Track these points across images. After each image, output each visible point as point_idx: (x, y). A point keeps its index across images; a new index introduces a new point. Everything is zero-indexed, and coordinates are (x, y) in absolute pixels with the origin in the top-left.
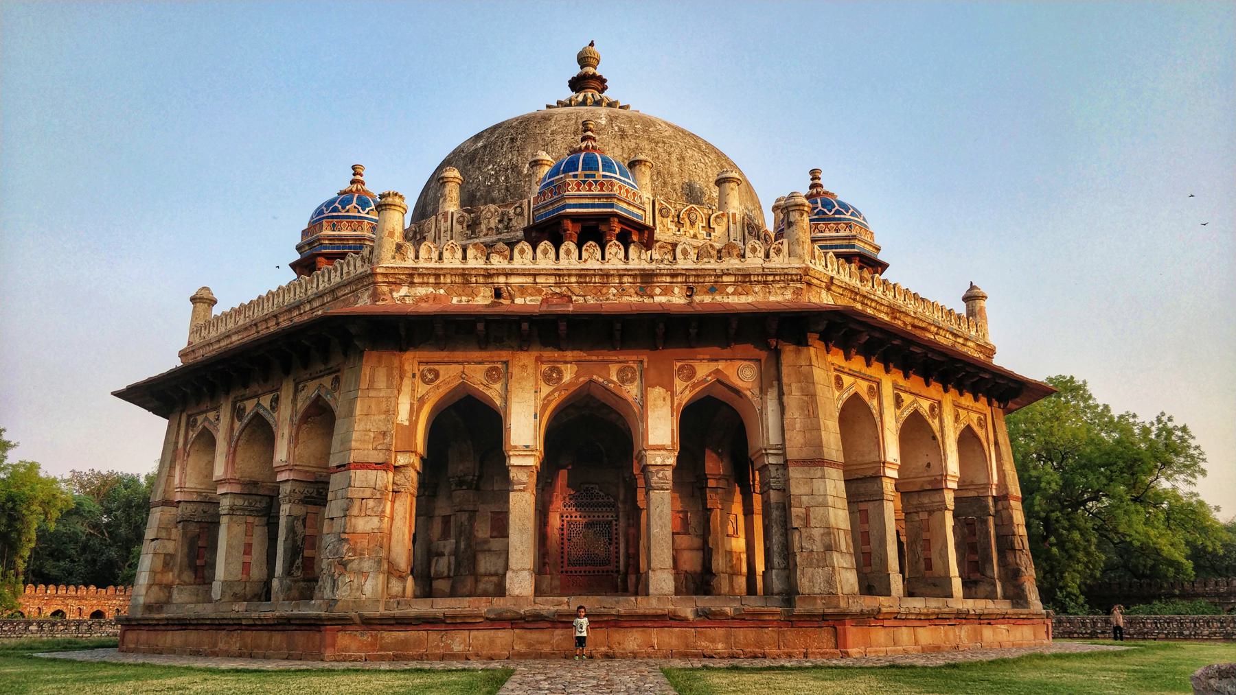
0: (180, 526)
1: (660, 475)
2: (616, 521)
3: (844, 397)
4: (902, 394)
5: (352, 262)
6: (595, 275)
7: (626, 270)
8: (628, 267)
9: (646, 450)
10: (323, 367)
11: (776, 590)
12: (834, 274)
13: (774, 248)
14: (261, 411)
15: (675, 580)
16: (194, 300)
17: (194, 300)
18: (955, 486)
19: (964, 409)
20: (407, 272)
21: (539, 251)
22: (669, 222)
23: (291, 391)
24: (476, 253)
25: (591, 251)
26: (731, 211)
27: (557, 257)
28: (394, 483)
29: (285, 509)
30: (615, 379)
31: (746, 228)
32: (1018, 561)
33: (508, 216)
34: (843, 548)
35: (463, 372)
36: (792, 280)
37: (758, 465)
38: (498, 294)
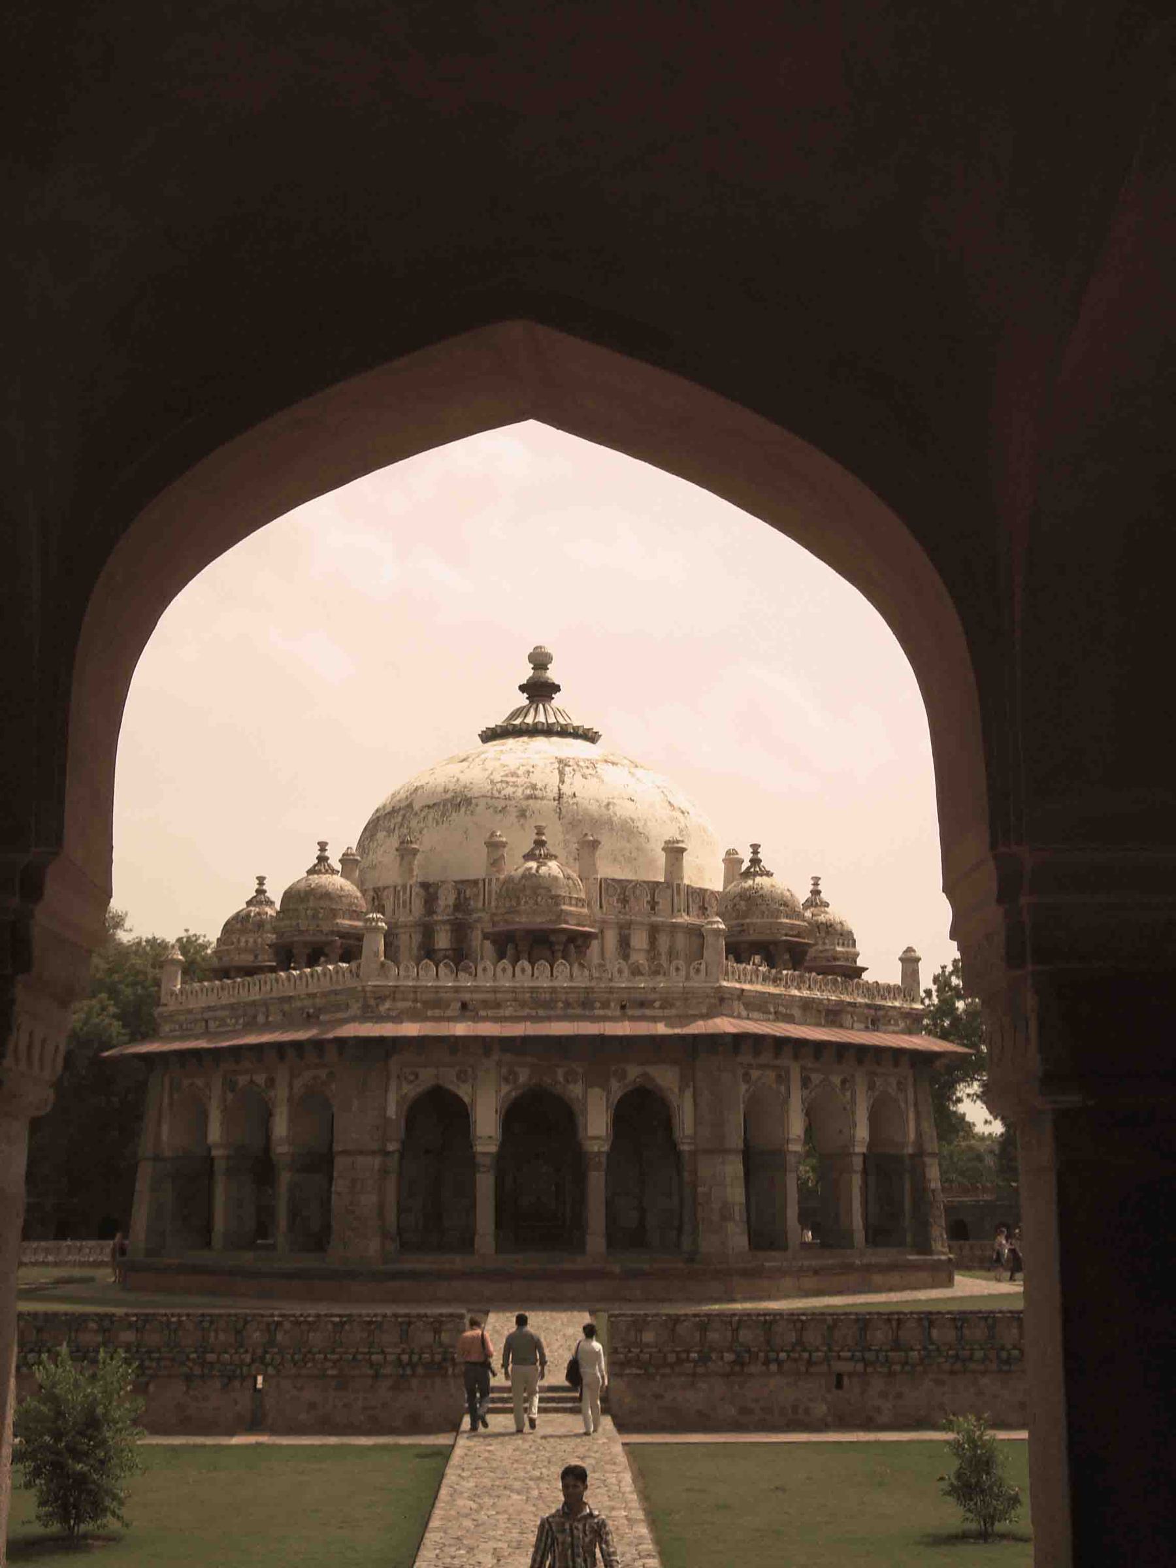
1: (597, 1159)
7: (571, 988)
8: (573, 984)
12: (747, 987)
18: (864, 1150)
21: (499, 970)
27: (514, 975)
29: (285, 1178)
34: (737, 1218)
37: (677, 1148)
38: (464, 1006)
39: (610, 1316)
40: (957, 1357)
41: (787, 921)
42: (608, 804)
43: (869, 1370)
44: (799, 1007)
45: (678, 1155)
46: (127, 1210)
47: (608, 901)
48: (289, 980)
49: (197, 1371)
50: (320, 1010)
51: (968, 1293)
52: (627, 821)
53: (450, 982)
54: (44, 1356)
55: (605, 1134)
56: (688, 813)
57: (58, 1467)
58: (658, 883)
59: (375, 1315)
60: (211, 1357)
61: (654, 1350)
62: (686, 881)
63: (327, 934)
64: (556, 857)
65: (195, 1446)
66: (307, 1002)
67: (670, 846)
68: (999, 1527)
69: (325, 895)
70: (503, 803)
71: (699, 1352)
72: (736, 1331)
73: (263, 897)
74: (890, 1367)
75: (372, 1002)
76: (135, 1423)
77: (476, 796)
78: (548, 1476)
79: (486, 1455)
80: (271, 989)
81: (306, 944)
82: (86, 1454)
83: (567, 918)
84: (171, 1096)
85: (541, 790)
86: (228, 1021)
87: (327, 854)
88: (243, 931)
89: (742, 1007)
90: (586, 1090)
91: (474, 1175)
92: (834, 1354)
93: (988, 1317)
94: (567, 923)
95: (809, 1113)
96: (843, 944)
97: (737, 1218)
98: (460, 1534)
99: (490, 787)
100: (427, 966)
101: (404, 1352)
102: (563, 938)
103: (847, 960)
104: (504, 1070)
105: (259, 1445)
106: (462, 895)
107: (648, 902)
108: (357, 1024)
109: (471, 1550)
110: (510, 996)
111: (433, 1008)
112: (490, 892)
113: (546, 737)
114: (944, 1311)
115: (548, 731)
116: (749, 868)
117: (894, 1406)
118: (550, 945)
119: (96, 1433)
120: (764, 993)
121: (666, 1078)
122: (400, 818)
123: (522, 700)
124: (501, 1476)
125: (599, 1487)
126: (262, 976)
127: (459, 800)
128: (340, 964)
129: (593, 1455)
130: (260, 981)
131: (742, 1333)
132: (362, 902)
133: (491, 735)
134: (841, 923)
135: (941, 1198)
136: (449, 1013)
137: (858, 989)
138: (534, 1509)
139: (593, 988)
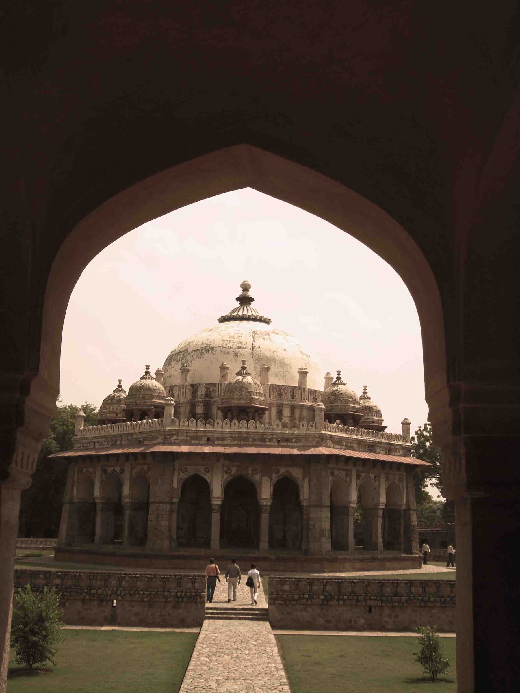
4: (361, 474)
5: (154, 423)
12: (334, 434)
14: (115, 473)
18: (383, 507)
22: (276, 394)
25: (243, 424)
27: (231, 426)
28: (172, 508)
29: (127, 513)
30: (251, 473)
31: (310, 393)
34: (327, 536)
35: (196, 469)
38: (209, 439)
39: (270, 578)
40: (422, 600)
41: (352, 405)
42: (274, 352)
43: (383, 604)
44: (357, 443)
45: (301, 507)
46: (58, 526)
48: (131, 425)
49: (87, 598)
50: (145, 439)
51: (428, 572)
52: (282, 360)
53: (202, 428)
54: (20, 590)
55: (269, 497)
56: (309, 356)
57: (25, 639)
58: (295, 387)
59: (166, 575)
60: (93, 591)
61: (289, 593)
62: (308, 386)
63: (149, 406)
64: (250, 374)
65: (86, 630)
66: (139, 436)
67: (301, 370)
68: (439, 676)
69: (149, 389)
70: (228, 350)
71: (308, 595)
72: (325, 586)
73: (121, 388)
74: (393, 604)
75: (168, 437)
76: (60, 619)
77: (216, 346)
78: (241, 648)
79: (214, 638)
80: (124, 430)
81: (139, 410)
82: (38, 633)
83: (254, 402)
84: (78, 476)
85: (245, 344)
86: (104, 443)
87: (149, 370)
88: (111, 404)
89: (331, 442)
90: (262, 478)
91: (211, 514)
92: (368, 597)
93: (436, 583)
94: (255, 404)
95: (360, 490)
96: (377, 416)
97: (327, 536)
98: (202, 672)
99: (222, 343)
100: (192, 422)
101: (178, 592)
102: (253, 410)
103: (378, 423)
104: (225, 468)
105: (114, 631)
106: (209, 391)
107: (290, 395)
108: (161, 446)
109: (206, 680)
110: (229, 435)
111: (195, 440)
112: (221, 389)
113: (247, 321)
114: (417, 580)
115: (248, 318)
116: (336, 381)
117: (394, 621)
118: (247, 413)
119: (42, 624)
120: (341, 437)
121: (297, 473)
122: (182, 356)
123: (237, 304)
124: (220, 647)
125: (263, 653)
126: (120, 424)
127: (208, 348)
128: (154, 419)
129: (261, 639)
130: (119, 426)
131: (327, 587)
132: (164, 392)
133: (223, 320)
134: (376, 407)
135: (417, 529)
136: (202, 442)
138: (235, 662)
139: (265, 433)
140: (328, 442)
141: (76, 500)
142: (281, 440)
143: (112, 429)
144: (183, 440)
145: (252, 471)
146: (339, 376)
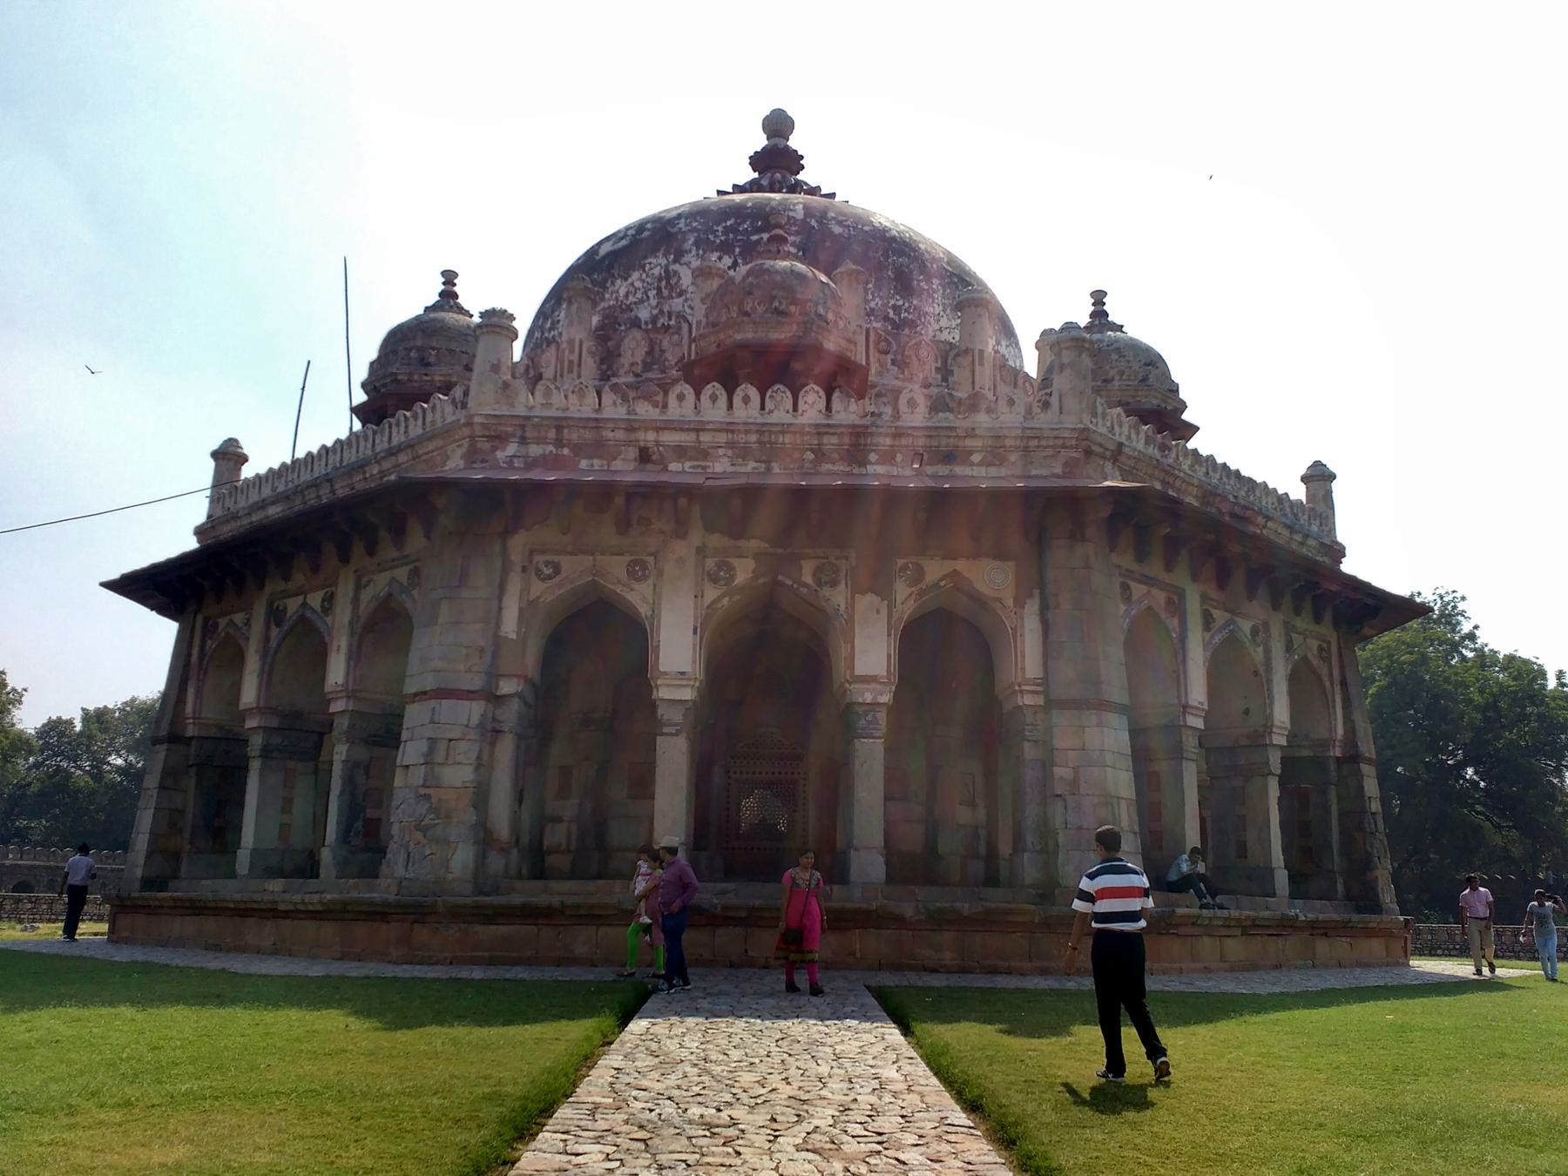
0: (193, 771)
1: (869, 718)
2: (805, 780)
3: (1133, 612)
4: (1216, 613)
5: (438, 406)
6: (783, 432)
7: (828, 425)
9: (850, 683)
10: (395, 554)
11: (1028, 880)
12: (1123, 439)
13: (1039, 401)
14: (308, 614)
15: (887, 863)
16: (215, 455)
17: (215, 455)
19: (1300, 633)
20: (517, 423)
22: (889, 361)
23: (351, 586)
24: (614, 397)
26: (979, 347)
27: (730, 406)
28: (494, 719)
29: (340, 753)
32: (1369, 849)
33: (660, 346)
35: (594, 566)
36: (1064, 447)
38: (644, 456)
47: (879, 360)
66: (386, 465)
90: (853, 597)
104: (710, 563)
106: (657, 349)
107: (937, 369)
111: (591, 458)
137: (1266, 497)
140: (1106, 470)
141: (191, 727)
142: (925, 457)
143: (309, 468)
144: (544, 456)
145: (817, 572)
146: (1099, 308)
